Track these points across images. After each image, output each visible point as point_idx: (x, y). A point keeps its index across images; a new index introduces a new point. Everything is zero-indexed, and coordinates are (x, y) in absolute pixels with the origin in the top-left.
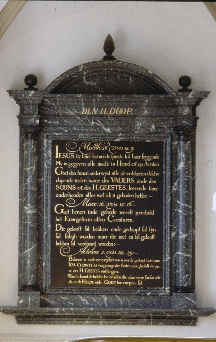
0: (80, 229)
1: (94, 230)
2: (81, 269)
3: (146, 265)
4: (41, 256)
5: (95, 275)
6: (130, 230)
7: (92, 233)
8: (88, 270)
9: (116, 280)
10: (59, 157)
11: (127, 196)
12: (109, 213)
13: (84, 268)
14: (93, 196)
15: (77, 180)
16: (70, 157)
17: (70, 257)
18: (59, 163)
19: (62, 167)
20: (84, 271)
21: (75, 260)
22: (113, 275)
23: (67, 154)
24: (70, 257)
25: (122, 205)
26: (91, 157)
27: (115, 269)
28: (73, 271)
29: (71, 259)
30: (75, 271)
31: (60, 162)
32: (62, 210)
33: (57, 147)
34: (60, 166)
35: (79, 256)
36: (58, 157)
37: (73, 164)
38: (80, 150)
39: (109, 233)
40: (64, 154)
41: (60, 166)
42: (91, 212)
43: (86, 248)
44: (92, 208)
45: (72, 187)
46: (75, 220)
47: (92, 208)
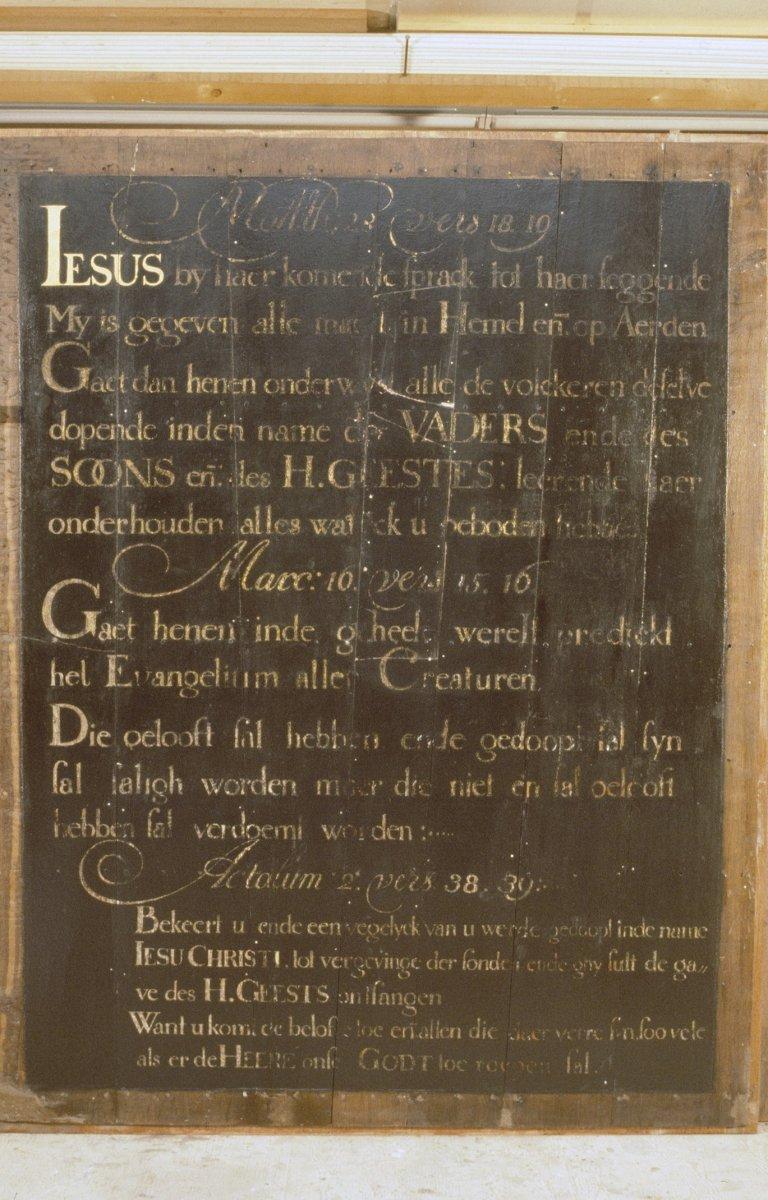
0: (202, 739)
1: (296, 740)
2: (215, 985)
3: (620, 957)
5: (303, 1020)
6: (521, 741)
7: (284, 762)
8: (258, 990)
9: (431, 1047)
10: (70, 282)
11: (503, 528)
12: (385, 632)
13: (233, 975)
15: (181, 427)
16: (140, 280)
17: (146, 911)
19: (84, 341)
20: (231, 992)
21: (175, 928)
22: (414, 1019)
23: (117, 258)
25: (472, 586)
27: (422, 982)
28: (160, 996)
29: (148, 923)
30: (177, 996)
31: (71, 309)
32: (91, 617)
33: (54, 213)
35: (200, 903)
36: (63, 278)
37: (155, 326)
38: (199, 231)
40: (99, 262)
41: (71, 336)
42: (273, 633)
44: (275, 607)
45: (153, 470)
46: (175, 678)
47: (275, 607)
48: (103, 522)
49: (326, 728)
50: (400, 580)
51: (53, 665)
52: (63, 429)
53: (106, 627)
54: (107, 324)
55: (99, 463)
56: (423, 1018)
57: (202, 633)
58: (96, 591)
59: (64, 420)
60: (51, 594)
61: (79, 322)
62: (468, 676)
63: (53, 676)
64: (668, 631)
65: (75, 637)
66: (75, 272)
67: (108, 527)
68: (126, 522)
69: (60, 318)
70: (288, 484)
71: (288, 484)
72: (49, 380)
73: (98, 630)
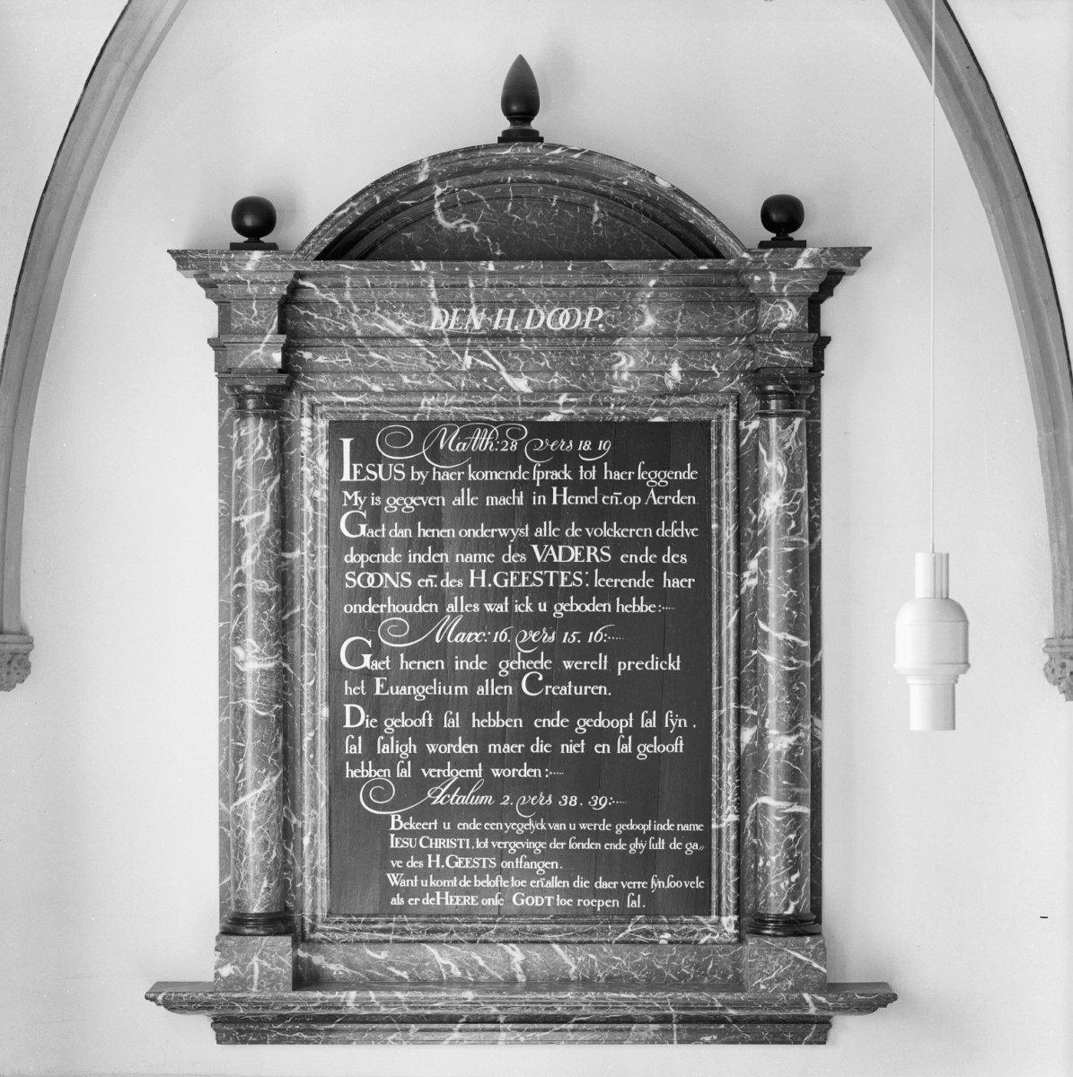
0: (427, 722)
1: (477, 723)
2: (434, 858)
3: (655, 841)
4: (295, 814)
5: (482, 877)
6: (600, 723)
7: (473, 735)
8: (457, 860)
9: (555, 891)
10: (355, 479)
11: (587, 608)
12: (526, 665)
13: (444, 852)
14: (473, 608)
17: (396, 818)
18: (354, 497)
20: (443, 862)
21: (412, 827)
22: (543, 876)
23: (380, 466)
24: (396, 818)
25: (572, 639)
26: (465, 477)
27: (547, 855)
29: (397, 824)
30: (413, 865)
31: (356, 493)
32: (367, 657)
33: (347, 442)
34: (356, 508)
35: (420, 815)
36: (352, 476)
37: (401, 502)
38: (424, 451)
39: (527, 735)
40: (371, 468)
41: (356, 508)
43: (449, 784)
44: (467, 651)
45: (400, 578)
46: (412, 690)
47: (467, 651)
49: (494, 716)
50: (533, 636)
52: (351, 556)
56: (549, 874)
57: (426, 665)
58: (369, 643)
62: (570, 686)
64: (678, 662)
68: (385, 606)
69: (350, 498)
70: (472, 585)
71: (472, 585)
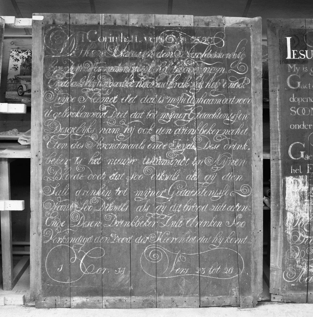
18: (293, 67)
31: (295, 65)
32: (302, 153)
33: (289, 39)
34: (295, 73)
36: (292, 56)
41: (295, 73)
48: (305, 126)
51: (292, 167)
52: (293, 99)
53: (307, 156)
54: (305, 69)
55: (304, 108)
58: (304, 145)
59: (293, 96)
60: (291, 147)
61: (297, 69)
63: (292, 170)
65: (298, 159)
66: (295, 55)
67: (306, 127)
69: (291, 68)
72: (289, 85)
73: (304, 157)
